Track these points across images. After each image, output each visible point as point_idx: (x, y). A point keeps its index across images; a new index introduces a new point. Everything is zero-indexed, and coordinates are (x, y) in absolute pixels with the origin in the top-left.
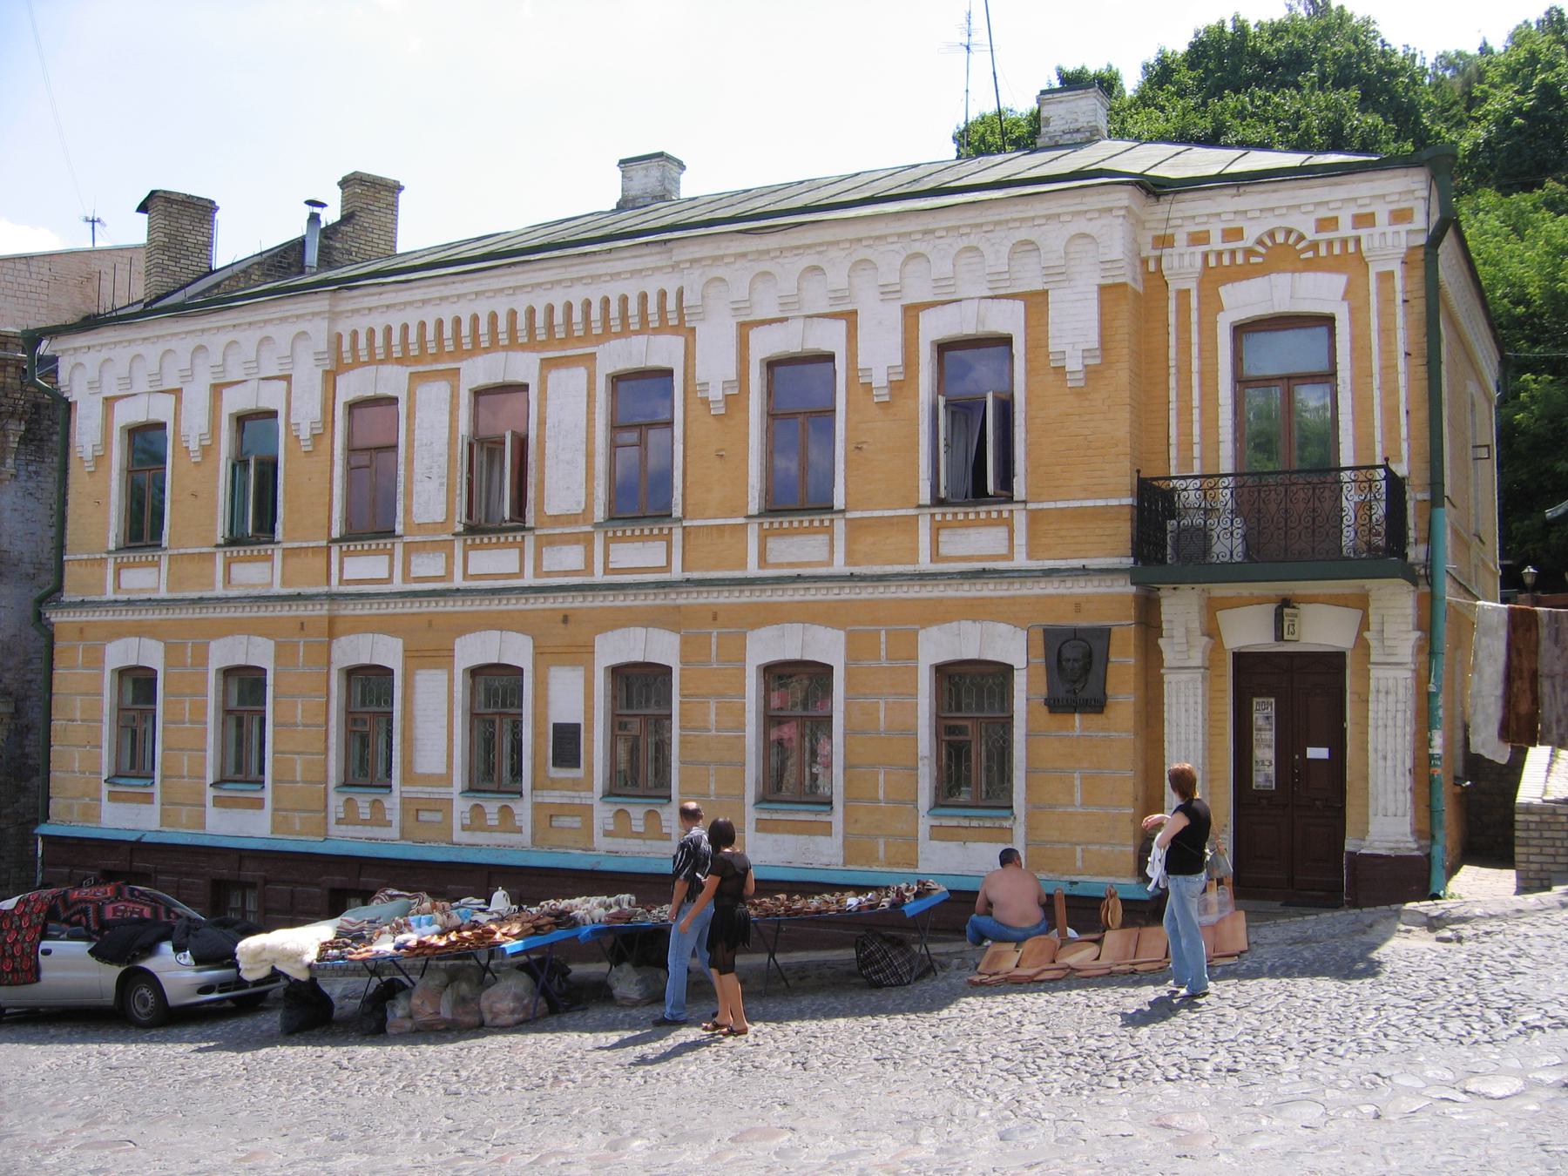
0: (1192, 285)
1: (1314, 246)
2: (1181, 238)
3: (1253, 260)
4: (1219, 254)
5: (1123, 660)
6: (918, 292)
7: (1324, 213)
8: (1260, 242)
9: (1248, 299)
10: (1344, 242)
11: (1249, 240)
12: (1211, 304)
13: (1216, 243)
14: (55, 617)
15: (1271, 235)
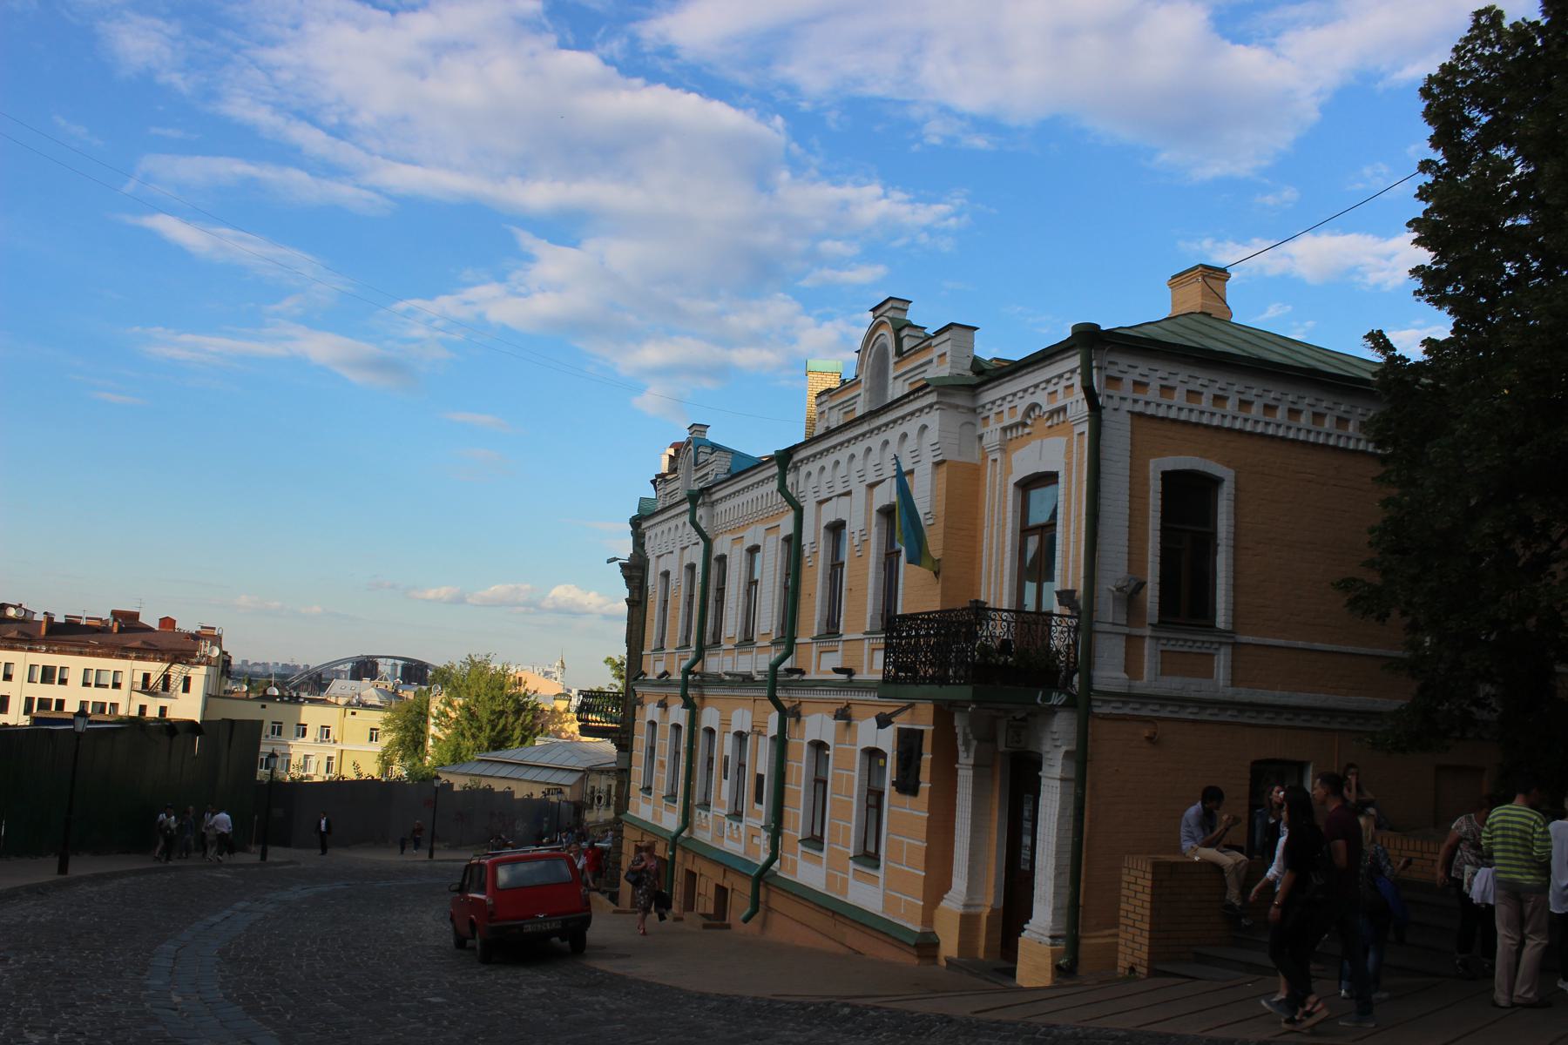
0: (997, 455)
1: (1052, 413)
2: (992, 416)
3: (1027, 430)
4: (1011, 427)
5: (927, 756)
6: (871, 479)
7: (1051, 388)
8: (1027, 414)
9: (1026, 462)
10: (1064, 409)
11: (1018, 418)
12: (1008, 470)
13: (1007, 421)
14: (637, 689)
15: (1033, 407)
